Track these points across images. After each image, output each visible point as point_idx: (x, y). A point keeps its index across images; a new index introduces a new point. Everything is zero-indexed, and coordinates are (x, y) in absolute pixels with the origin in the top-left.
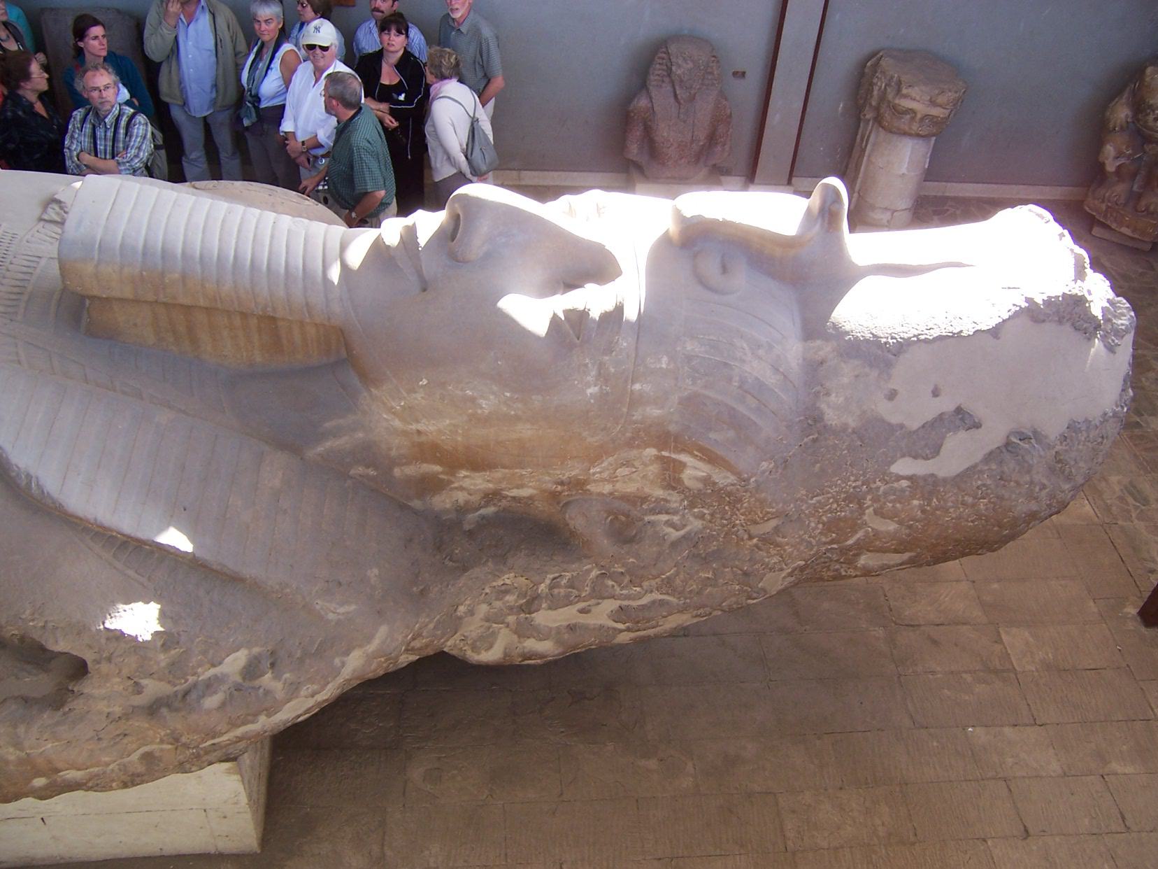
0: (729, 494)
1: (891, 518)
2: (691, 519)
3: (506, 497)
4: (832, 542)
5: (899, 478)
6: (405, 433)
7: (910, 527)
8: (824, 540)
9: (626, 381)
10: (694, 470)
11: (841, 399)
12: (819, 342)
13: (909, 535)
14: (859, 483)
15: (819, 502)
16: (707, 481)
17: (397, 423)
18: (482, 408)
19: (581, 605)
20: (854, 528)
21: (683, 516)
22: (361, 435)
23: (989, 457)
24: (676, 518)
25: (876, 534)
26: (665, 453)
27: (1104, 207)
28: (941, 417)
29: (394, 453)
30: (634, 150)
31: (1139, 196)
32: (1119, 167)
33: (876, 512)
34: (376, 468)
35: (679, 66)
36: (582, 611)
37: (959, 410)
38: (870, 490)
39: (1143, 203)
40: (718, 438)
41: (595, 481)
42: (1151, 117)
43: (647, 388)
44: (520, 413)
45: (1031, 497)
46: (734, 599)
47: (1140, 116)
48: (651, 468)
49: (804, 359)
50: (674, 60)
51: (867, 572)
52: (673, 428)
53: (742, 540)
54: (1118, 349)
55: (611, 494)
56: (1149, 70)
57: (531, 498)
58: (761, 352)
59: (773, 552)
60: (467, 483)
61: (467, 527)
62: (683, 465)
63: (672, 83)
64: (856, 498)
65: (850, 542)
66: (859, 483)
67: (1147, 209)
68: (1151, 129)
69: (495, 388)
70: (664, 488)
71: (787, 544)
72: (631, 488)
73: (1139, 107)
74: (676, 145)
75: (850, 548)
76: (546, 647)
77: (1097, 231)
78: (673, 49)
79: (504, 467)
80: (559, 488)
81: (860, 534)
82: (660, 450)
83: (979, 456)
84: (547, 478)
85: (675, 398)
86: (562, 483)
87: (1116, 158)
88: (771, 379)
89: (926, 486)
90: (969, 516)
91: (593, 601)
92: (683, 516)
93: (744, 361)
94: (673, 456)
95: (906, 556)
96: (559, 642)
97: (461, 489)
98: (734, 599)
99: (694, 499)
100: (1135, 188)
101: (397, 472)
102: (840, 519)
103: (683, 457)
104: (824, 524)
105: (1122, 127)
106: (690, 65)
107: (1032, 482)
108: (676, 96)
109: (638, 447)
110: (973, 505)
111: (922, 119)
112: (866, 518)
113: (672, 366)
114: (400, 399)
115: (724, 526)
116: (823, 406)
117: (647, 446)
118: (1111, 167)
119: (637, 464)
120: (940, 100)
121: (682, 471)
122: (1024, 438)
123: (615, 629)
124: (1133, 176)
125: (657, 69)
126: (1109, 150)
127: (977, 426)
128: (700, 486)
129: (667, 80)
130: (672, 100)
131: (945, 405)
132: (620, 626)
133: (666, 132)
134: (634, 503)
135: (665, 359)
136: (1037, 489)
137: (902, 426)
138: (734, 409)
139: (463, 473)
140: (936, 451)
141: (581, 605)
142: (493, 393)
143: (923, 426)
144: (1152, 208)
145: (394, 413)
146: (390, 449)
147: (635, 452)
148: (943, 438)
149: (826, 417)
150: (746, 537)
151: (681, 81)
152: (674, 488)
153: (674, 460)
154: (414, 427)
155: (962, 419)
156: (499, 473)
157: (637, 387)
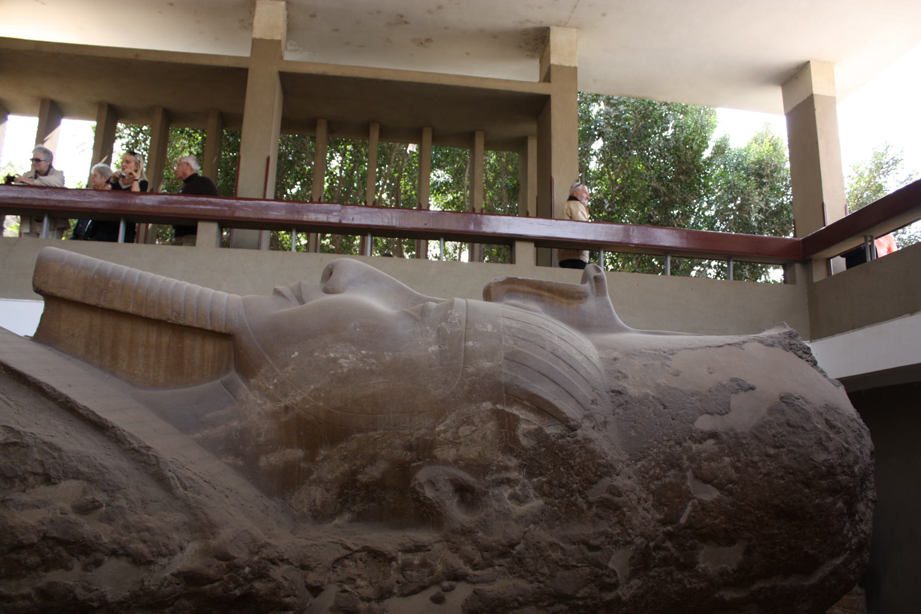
0: (562, 448)
6: (274, 415)
7: (731, 493)
10: (528, 421)
11: (638, 379)
14: (672, 443)
15: (643, 466)
16: (538, 434)
18: (342, 367)
19: (434, 591)
21: (524, 486)
22: (235, 424)
23: (771, 411)
26: (499, 407)
36: (438, 600)
40: (545, 391)
43: (478, 345)
44: (374, 367)
48: (489, 425)
52: (503, 379)
53: (583, 511)
55: (456, 462)
62: (516, 419)
64: (673, 463)
66: (672, 443)
82: (494, 405)
86: (409, 448)
94: (507, 410)
103: (515, 411)
104: (653, 493)
117: (484, 401)
119: (476, 420)
137: (693, 394)
142: (353, 353)
143: (710, 391)
145: (267, 396)
146: (259, 435)
147: (473, 407)
150: (585, 507)
153: (509, 414)
157: (470, 343)
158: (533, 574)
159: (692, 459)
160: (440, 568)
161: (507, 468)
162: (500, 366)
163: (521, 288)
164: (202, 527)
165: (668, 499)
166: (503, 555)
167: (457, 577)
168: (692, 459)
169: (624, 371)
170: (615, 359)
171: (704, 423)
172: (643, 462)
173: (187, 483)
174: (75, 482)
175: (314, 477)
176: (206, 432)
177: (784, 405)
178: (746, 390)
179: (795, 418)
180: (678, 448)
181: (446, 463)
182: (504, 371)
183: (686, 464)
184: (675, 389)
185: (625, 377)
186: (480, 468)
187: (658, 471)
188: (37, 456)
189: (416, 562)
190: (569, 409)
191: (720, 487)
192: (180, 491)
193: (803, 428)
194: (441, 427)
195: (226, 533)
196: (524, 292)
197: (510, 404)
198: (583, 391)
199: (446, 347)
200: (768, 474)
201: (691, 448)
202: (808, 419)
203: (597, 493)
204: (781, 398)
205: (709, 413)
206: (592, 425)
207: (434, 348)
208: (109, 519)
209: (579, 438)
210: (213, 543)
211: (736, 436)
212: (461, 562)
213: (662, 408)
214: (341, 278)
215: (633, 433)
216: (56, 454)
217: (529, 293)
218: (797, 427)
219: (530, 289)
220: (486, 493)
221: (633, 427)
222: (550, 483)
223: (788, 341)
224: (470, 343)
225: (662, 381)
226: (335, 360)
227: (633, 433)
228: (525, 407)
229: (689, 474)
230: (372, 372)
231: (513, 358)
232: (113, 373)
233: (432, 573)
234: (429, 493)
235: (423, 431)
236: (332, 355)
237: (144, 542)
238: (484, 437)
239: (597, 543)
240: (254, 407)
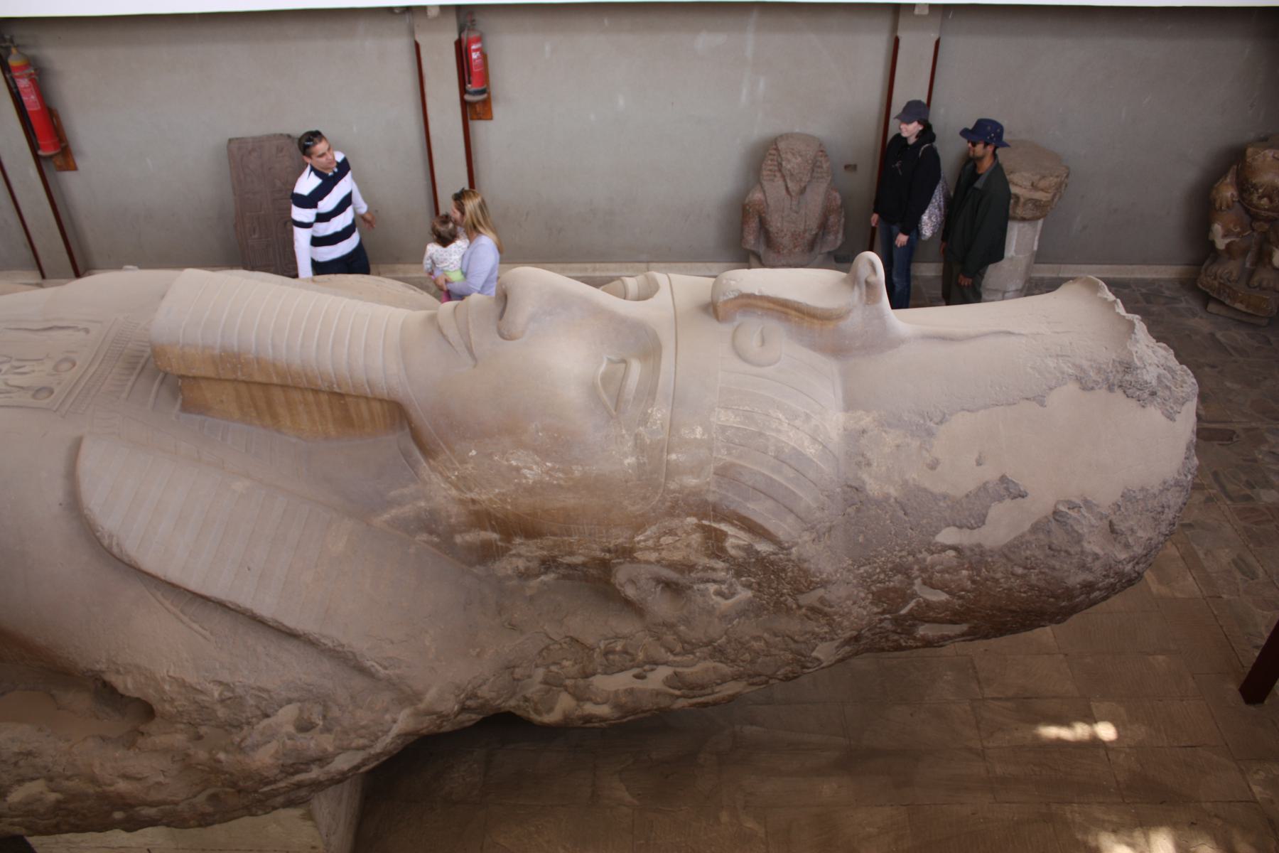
0: (772, 563)
1: (941, 589)
2: (739, 588)
3: (562, 564)
4: (883, 613)
5: (945, 548)
6: (462, 502)
7: (961, 597)
8: (876, 610)
9: (662, 451)
10: (736, 538)
11: (884, 468)
12: (860, 413)
13: (961, 606)
14: (904, 553)
15: (866, 571)
16: (749, 549)
17: (454, 492)
18: (526, 478)
19: (636, 671)
20: (906, 598)
21: (731, 585)
22: (423, 504)
23: (1035, 529)
24: (724, 587)
25: (929, 605)
26: (705, 522)
27: (1216, 283)
28: (984, 487)
29: (453, 520)
30: (751, 241)
31: (1251, 274)
32: (1228, 246)
33: (924, 583)
34: (439, 535)
35: (789, 161)
36: (637, 677)
37: (1003, 479)
38: (917, 561)
39: (1256, 279)
40: (757, 510)
41: (640, 549)
42: (1255, 197)
43: (682, 458)
44: (562, 482)
45: (1083, 567)
46: (789, 668)
47: (1245, 195)
49: (845, 430)
51: (928, 643)
52: (711, 498)
54: (1178, 417)
55: (658, 562)
56: (1250, 151)
57: (584, 564)
58: (798, 423)
59: (823, 622)
60: (523, 550)
61: (529, 593)
62: (725, 534)
63: (783, 177)
65: (903, 612)
66: (904, 553)
67: (1260, 286)
68: (1256, 207)
69: (538, 459)
70: (709, 556)
71: (836, 613)
72: (677, 556)
73: (1244, 186)
74: (789, 234)
75: (905, 617)
76: (604, 710)
77: (1212, 307)
78: (782, 145)
79: (555, 535)
80: (608, 556)
81: (912, 604)
83: (1027, 526)
84: (595, 546)
85: (712, 468)
86: (609, 551)
87: (1225, 236)
88: (811, 450)
89: (974, 558)
90: (1021, 586)
91: (647, 667)
92: (731, 585)
93: (779, 431)
94: (715, 525)
95: (964, 627)
96: (617, 706)
97: (519, 556)
98: (789, 668)
99: (739, 569)
100: (1248, 265)
101: (458, 539)
102: (888, 589)
103: (723, 527)
104: (873, 593)
105: (1228, 207)
107: (1083, 552)
108: (787, 188)
109: (679, 516)
110: (1023, 576)
111: (1025, 204)
112: (916, 588)
113: (705, 437)
114: (454, 469)
115: (772, 595)
116: (865, 477)
117: (689, 515)
118: (1221, 244)
119: (679, 532)
120: (1042, 184)
121: (724, 540)
122: (1073, 506)
123: (672, 695)
124: (1244, 253)
126: (1217, 228)
127: (1023, 495)
128: (742, 554)
129: (778, 174)
130: (784, 192)
131: (989, 474)
132: (677, 692)
134: (682, 572)
135: (699, 430)
136: (1089, 559)
137: (945, 497)
138: (771, 479)
139: (518, 540)
140: (981, 520)
141: (636, 671)
142: (537, 463)
143: (967, 496)
144: (1265, 284)
146: (449, 517)
148: (988, 507)
149: (868, 487)
152: (719, 557)
153: (716, 529)
154: (469, 495)
155: (1007, 489)
156: (549, 541)
157: (673, 457)
158: (733, 661)
159: (923, 570)
160: (641, 656)
161: (714, 569)
162: (708, 483)
163: (759, 303)
164: (408, 697)
165: (888, 598)
166: (707, 645)
167: (656, 663)
168: (923, 570)
169: (869, 454)
170: (864, 432)
171: (948, 536)
172: (867, 568)
173: (386, 664)
174: (290, 706)
175: (513, 552)
176: (394, 512)
177: (1053, 525)
178: (1015, 498)
179: (1059, 538)
180: (911, 558)
181: (648, 562)
182: (712, 488)
183: (915, 572)
184: (925, 490)
185: (869, 464)
186: (688, 567)
187: (882, 576)
188: (252, 702)
189: (619, 648)
190: (784, 527)
191: (950, 593)
192: (382, 672)
193: (1066, 552)
194: (641, 537)
195: (431, 695)
196: (763, 308)
197: (719, 522)
198: (807, 499)
199: (645, 460)
200: (1009, 589)
201: (925, 560)
202: (1079, 539)
203: (810, 598)
204: (1055, 513)
205: (955, 525)
206: (814, 535)
207: (630, 460)
208: (327, 730)
209: (793, 557)
210: (422, 706)
211: (982, 554)
212: (663, 650)
213: (901, 513)
214: (522, 312)
215: (861, 539)
216: (265, 695)
217: (769, 309)
218: (1059, 551)
219: (771, 305)
220: (690, 588)
221: (862, 532)
222: (759, 584)
223: (1119, 376)
224: (673, 457)
225: (912, 476)
226: (518, 469)
227: (861, 539)
228: (735, 525)
229: (918, 581)
230: (560, 486)
231: (725, 473)
233: (633, 660)
234: (630, 592)
235: (620, 541)
236: (514, 463)
237: (362, 737)
238: (688, 546)
239: (801, 639)
240: (438, 490)
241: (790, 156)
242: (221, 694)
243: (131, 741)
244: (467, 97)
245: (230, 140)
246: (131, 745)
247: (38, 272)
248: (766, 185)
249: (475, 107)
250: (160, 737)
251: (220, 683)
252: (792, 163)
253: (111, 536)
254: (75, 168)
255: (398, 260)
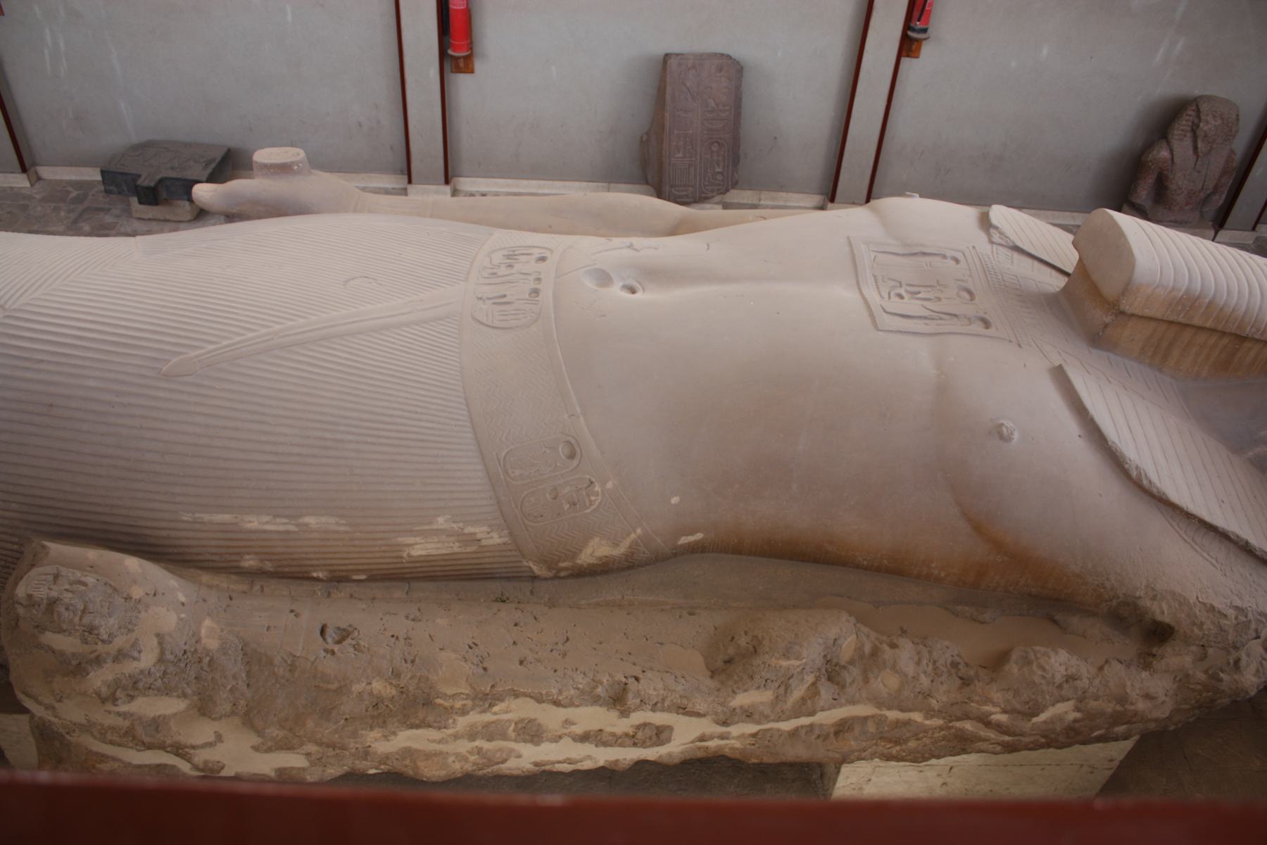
30: (1143, 194)
50: (1203, 117)
78: (1204, 107)
106: (1219, 122)
125: (1183, 124)
129: (1189, 134)
130: (1191, 152)
133: (1180, 182)
151: (1206, 136)
232: (1160, 370)
241: (1210, 118)
242: (1236, 618)
243: (1146, 661)
244: (910, 33)
245: (667, 56)
246: (1147, 666)
247: (406, 177)
248: (1176, 144)
249: (908, 46)
250: (1176, 658)
251: (1237, 608)
252: (1209, 125)
253: (1137, 468)
254: (472, 72)
255: (782, 188)
